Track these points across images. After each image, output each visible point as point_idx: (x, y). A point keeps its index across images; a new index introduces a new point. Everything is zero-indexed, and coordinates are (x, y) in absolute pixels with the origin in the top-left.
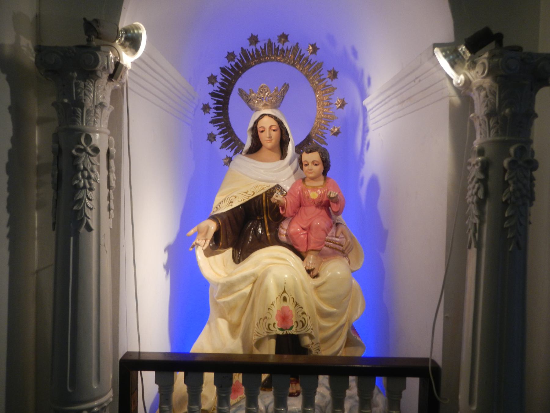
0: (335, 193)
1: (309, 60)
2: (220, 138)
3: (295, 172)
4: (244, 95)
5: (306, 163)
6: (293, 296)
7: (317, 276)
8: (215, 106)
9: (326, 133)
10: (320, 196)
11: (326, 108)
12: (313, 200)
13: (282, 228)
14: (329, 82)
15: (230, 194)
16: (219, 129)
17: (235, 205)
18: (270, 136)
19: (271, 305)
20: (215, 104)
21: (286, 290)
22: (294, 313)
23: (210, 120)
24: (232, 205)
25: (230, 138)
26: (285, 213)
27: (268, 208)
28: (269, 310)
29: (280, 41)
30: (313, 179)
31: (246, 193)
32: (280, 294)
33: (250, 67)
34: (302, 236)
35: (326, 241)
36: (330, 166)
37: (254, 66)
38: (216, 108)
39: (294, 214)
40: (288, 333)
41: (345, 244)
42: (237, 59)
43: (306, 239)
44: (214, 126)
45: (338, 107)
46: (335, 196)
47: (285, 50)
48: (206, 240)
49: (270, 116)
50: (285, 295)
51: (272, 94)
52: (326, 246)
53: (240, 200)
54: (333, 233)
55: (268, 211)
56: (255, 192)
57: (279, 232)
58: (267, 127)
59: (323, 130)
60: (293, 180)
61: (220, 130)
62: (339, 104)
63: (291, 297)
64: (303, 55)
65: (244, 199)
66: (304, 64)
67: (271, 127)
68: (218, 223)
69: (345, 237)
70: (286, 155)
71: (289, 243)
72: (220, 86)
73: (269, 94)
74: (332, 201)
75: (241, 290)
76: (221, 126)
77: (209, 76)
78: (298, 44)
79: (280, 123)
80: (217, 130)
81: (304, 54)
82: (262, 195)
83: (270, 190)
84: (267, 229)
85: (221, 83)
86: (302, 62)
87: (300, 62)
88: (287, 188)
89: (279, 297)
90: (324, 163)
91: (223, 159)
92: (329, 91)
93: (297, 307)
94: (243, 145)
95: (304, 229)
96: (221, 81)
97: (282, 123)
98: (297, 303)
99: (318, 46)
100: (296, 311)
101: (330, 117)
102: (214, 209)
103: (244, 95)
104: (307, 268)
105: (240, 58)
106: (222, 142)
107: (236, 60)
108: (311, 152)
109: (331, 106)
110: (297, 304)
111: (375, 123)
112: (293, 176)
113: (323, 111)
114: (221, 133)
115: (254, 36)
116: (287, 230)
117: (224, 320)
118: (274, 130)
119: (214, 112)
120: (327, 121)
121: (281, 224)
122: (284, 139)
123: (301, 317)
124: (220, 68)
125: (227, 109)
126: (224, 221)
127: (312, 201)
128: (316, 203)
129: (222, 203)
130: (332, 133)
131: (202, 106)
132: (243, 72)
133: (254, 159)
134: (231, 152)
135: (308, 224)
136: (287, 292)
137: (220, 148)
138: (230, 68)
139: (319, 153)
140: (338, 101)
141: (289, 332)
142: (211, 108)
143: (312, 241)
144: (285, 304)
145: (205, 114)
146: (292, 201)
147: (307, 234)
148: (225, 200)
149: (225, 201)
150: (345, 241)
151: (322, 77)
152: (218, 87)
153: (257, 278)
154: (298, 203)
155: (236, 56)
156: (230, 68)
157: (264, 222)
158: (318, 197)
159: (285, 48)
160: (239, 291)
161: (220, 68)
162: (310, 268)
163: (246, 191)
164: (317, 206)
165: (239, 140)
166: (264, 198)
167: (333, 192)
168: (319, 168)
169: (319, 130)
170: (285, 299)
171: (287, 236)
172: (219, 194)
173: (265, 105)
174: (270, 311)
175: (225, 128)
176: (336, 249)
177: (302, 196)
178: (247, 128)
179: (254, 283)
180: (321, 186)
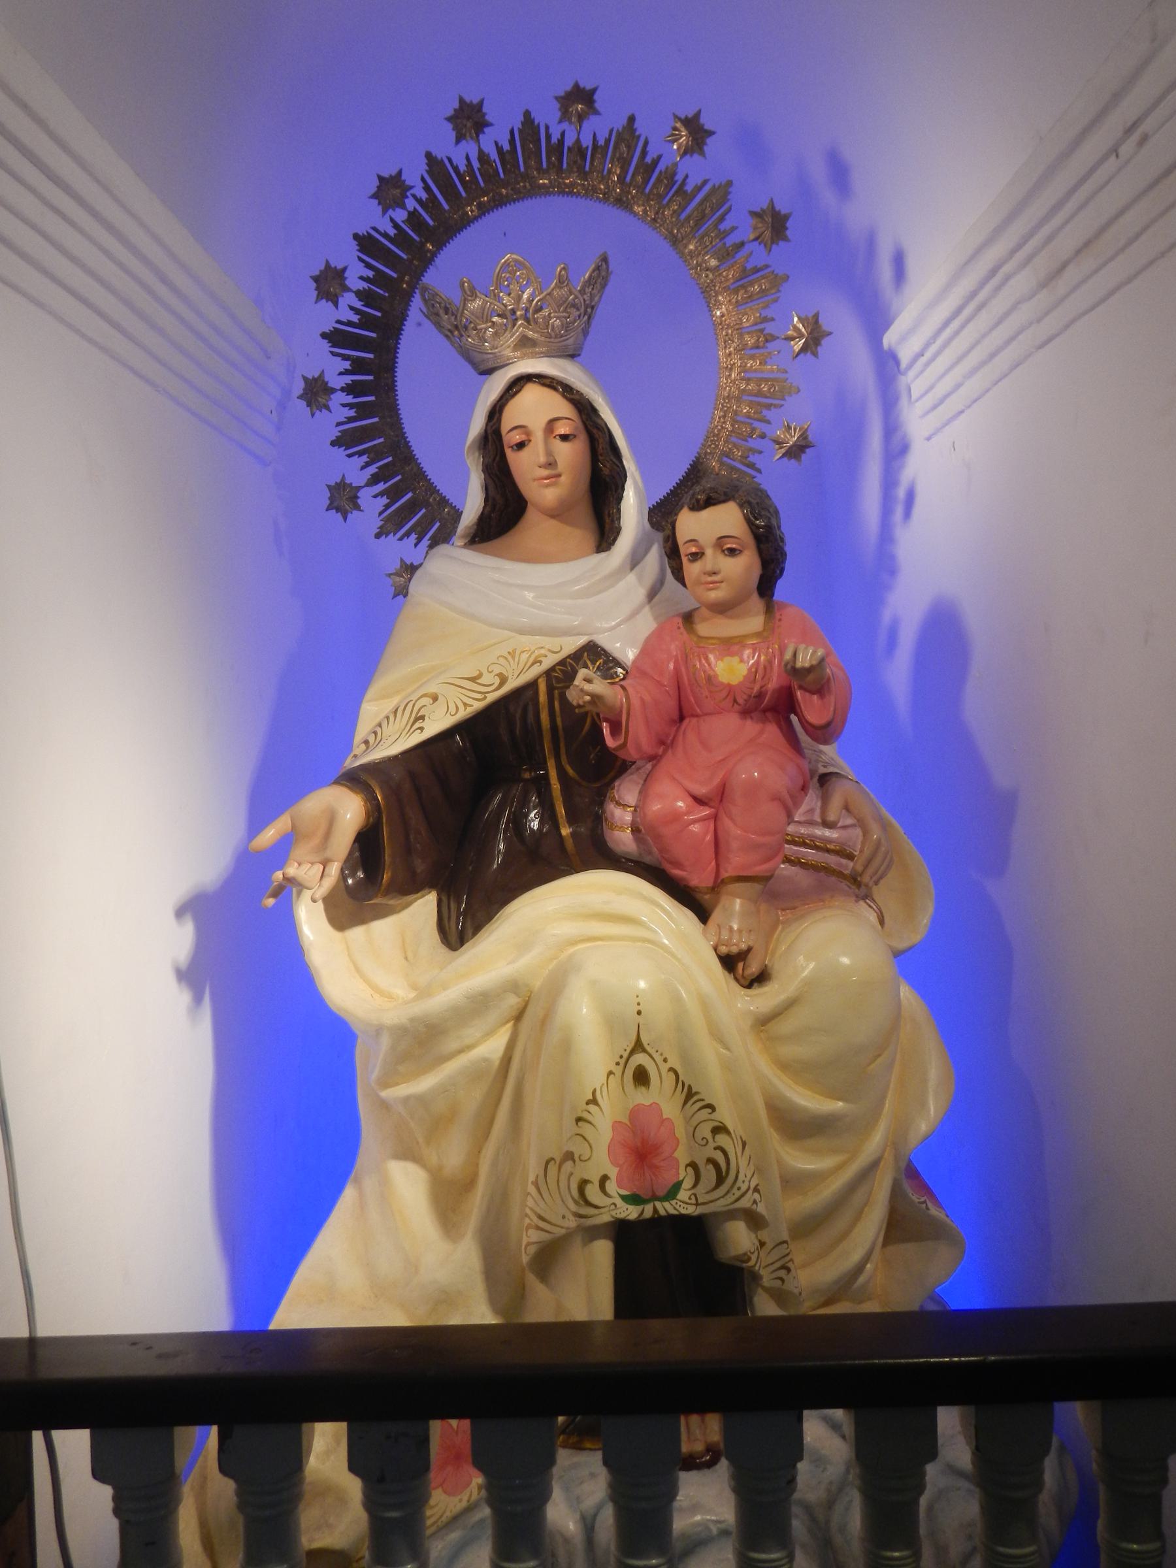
0: (814, 652)
1: (679, 178)
2: (375, 496)
3: (652, 594)
4: (442, 312)
5: (694, 550)
6: (674, 1062)
7: (761, 978)
8: (348, 379)
9: (761, 452)
11: (753, 357)
12: (730, 688)
13: (618, 804)
14: (757, 255)
15: (413, 692)
16: (367, 465)
17: (435, 726)
18: (551, 459)
19: (588, 1103)
21: (645, 1040)
22: (680, 1132)
23: (335, 433)
24: (421, 729)
25: (410, 495)
26: (624, 745)
27: (561, 733)
28: (580, 1124)
29: (565, 115)
30: (722, 609)
31: (473, 679)
32: (621, 1057)
33: (465, 223)
34: (695, 828)
35: (788, 842)
36: (784, 555)
37: (476, 218)
38: (350, 389)
39: (660, 751)
40: (662, 1212)
41: (861, 851)
43: (709, 837)
44: (349, 456)
45: (797, 348)
46: (814, 662)
47: (587, 147)
48: (325, 863)
49: (547, 381)
50: (640, 1059)
51: (549, 294)
52: (787, 860)
53: (453, 709)
54: (811, 811)
55: (562, 745)
56: (505, 673)
57: (606, 819)
58: (537, 426)
59: (747, 441)
60: (646, 624)
61: (373, 469)
62: (801, 336)
63: (664, 1068)
64: (656, 162)
65: (465, 705)
66: (661, 197)
67: (551, 423)
68: (370, 797)
69: (861, 823)
70: (617, 531)
71: (647, 859)
72: (358, 305)
73: (533, 295)
74: (801, 687)
75: (470, 1047)
76: (375, 455)
77: (317, 273)
78: (632, 119)
79: (585, 409)
80: (362, 468)
81: (660, 157)
82: (532, 685)
83: (562, 663)
84: (561, 810)
85: (360, 294)
86: (651, 190)
87: (647, 191)
88: (630, 655)
89: (618, 1070)
90: (762, 546)
91: (389, 575)
92: (762, 291)
93: (691, 1108)
94: (457, 515)
95: (699, 801)
96: (363, 285)
97: (595, 411)
98: (690, 1087)
99: (707, 122)
100: (688, 1120)
101: (769, 389)
102: (358, 748)
103: (442, 312)
104: (723, 950)
108: (709, 502)
110: (690, 1094)
111: (935, 407)
112: (647, 609)
113: (743, 369)
114: (375, 480)
115: (470, 106)
116: (635, 810)
117: (411, 1167)
118: (565, 438)
119: (344, 405)
120: (759, 404)
121: (613, 788)
122: (606, 471)
123: (712, 1145)
124: (356, 237)
125: (391, 388)
126: (394, 793)
127: (724, 693)
128: (740, 701)
129: (385, 724)
130: (783, 451)
131: (299, 387)
132: (440, 245)
134: (416, 545)
135: (716, 781)
136: (648, 1048)
137: (378, 536)
138: (392, 232)
139: (741, 506)
140: (796, 329)
141: (666, 1208)
142: (333, 391)
143: (735, 845)
144: (642, 1097)
145: (313, 415)
146: (647, 698)
147: (715, 817)
148: (395, 712)
149: (395, 716)
150: (861, 838)
151: (730, 241)
152: (352, 308)
153: (529, 997)
154: (672, 704)
155: (412, 187)
156: (392, 232)
157: (548, 784)
158: (745, 677)
159: (587, 142)
160: (461, 1051)
161: (356, 237)
162: (734, 950)
163: (475, 674)
164: (746, 713)
165: (444, 501)
166: (543, 697)
167: (806, 648)
169: (734, 439)
170: (641, 1077)
171: (636, 830)
172: (371, 693)
173: (524, 343)
174: (585, 1129)
175: (390, 459)
176: (827, 870)
177: (685, 678)
178: (465, 444)
180: (758, 634)
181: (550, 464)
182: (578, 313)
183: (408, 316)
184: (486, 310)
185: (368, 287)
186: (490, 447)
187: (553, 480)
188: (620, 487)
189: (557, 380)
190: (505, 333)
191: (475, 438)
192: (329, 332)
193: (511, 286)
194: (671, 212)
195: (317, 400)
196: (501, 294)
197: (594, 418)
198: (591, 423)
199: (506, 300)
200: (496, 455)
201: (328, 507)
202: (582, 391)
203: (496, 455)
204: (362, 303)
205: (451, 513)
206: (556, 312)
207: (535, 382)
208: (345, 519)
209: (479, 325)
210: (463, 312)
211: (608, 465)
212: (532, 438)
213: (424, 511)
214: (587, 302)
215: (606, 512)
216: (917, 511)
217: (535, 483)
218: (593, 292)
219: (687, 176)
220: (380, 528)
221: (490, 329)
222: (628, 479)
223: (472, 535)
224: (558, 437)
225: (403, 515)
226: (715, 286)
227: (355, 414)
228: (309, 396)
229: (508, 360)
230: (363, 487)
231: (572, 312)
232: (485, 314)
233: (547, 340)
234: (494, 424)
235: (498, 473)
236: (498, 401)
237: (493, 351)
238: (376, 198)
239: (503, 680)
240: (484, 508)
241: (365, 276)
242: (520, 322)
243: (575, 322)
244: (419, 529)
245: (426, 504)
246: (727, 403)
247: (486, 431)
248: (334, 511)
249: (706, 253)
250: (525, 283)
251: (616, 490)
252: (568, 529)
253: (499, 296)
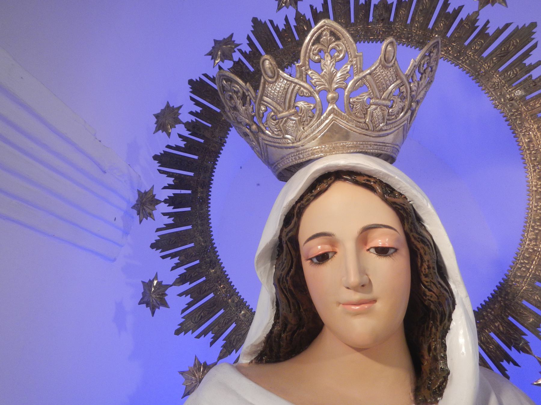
1: (480, 24)
2: (180, 295)
8: (171, 192)
16: (177, 266)
20: (170, 187)
23: (155, 237)
25: (212, 295)
38: (170, 201)
42: (240, 50)
44: (163, 257)
61: (181, 270)
72: (186, 133)
77: (159, 111)
80: (173, 269)
81: (461, 8)
85: (188, 126)
87: (449, 35)
103: (239, 103)
105: (248, 49)
106: (183, 311)
107: (237, 56)
114: (182, 280)
118: (382, 251)
119: (164, 214)
124: (191, 82)
125: (205, 201)
134: (212, 344)
137: (178, 332)
142: (158, 202)
152: (180, 136)
161: (191, 82)
175: (198, 262)
181: (363, 286)
182: (402, 104)
183: (225, 142)
184: (290, 91)
185: (196, 119)
186: (284, 257)
187: (366, 306)
188: (447, 315)
189: (375, 178)
190: (311, 120)
191: (266, 246)
192: (160, 154)
193: (323, 62)
194: (473, 51)
195: (145, 209)
196: (310, 72)
197: (420, 229)
198: (417, 236)
199: (315, 77)
200: (291, 267)
201: (140, 301)
202: (407, 195)
203: (291, 267)
204: (190, 133)
205: (247, 315)
206: (378, 98)
207: (346, 180)
208: (153, 313)
209: (280, 112)
210: (261, 99)
211: (435, 289)
212: (337, 250)
213: (222, 311)
214: (413, 93)
215: (425, 347)
217: (341, 307)
218: (420, 83)
219: (488, 22)
220: (181, 324)
221: (293, 118)
222: (456, 307)
223: (259, 352)
224: (373, 250)
225: (202, 314)
226: (521, 114)
227: (173, 222)
228: (139, 205)
229: (313, 154)
230: (171, 286)
231: (395, 100)
232: (289, 96)
233: (365, 132)
234: (289, 232)
235: (292, 288)
236: (297, 202)
237: (295, 145)
238: (210, 55)
240: (274, 326)
241: (194, 111)
242: (330, 108)
243: (398, 113)
244: (217, 328)
245: (226, 306)
246: (538, 226)
247: (280, 238)
248: (145, 305)
249: (510, 86)
250: (341, 56)
251: (441, 321)
252: (376, 367)
253: (307, 74)
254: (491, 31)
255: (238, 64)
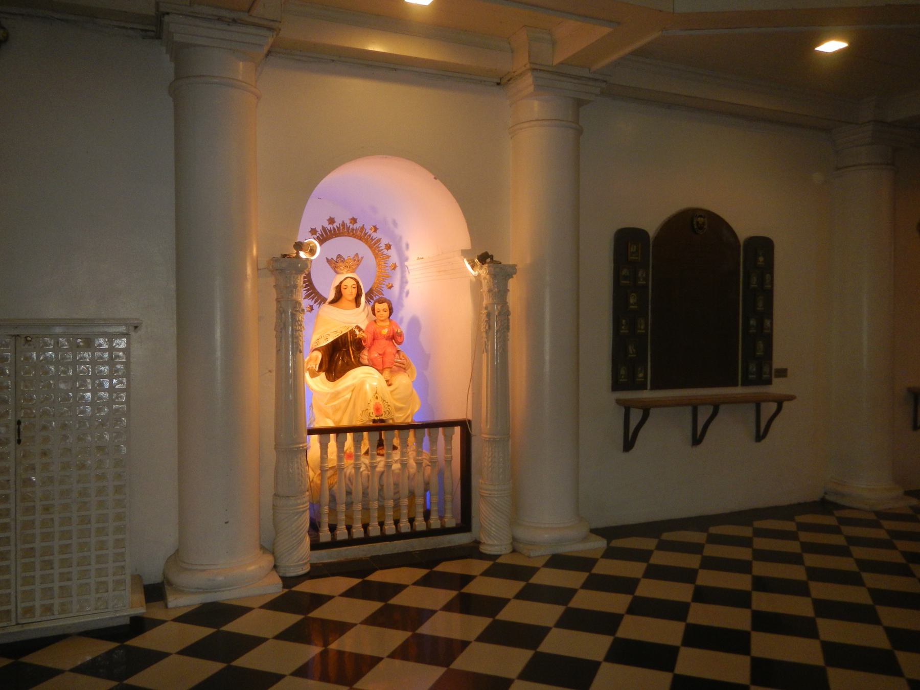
3: (367, 316)
6: (382, 396)
10: (388, 332)
12: (384, 335)
14: (385, 252)
22: (383, 406)
30: (382, 321)
43: (382, 361)
50: (376, 395)
52: (395, 365)
64: (368, 233)
78: (364, 225)
79: (357, 282)
82: (347, 333)
88: (363, 327)
95: (380, 354)
107: (318, 235)
108: (382, 303)
109: (387, 268)
110: (384, 400)
118: (354, 288)
133: (334, 306)
135: (383, 351)
141: (381, 418)
144: (377, 401)
147: (383, 358)
154: (373, 337)
159: (355, 228)
160: (343, 397)
164: (386, 339)
168: (387, 313)
170: (377, 398)
171: (368, 360)
176: (400, 367)
179: (353, 391)
216: (410, 295)
239: (342, 332)
245: (314, 293)
254: (373, 238)
255: (318, 237)
